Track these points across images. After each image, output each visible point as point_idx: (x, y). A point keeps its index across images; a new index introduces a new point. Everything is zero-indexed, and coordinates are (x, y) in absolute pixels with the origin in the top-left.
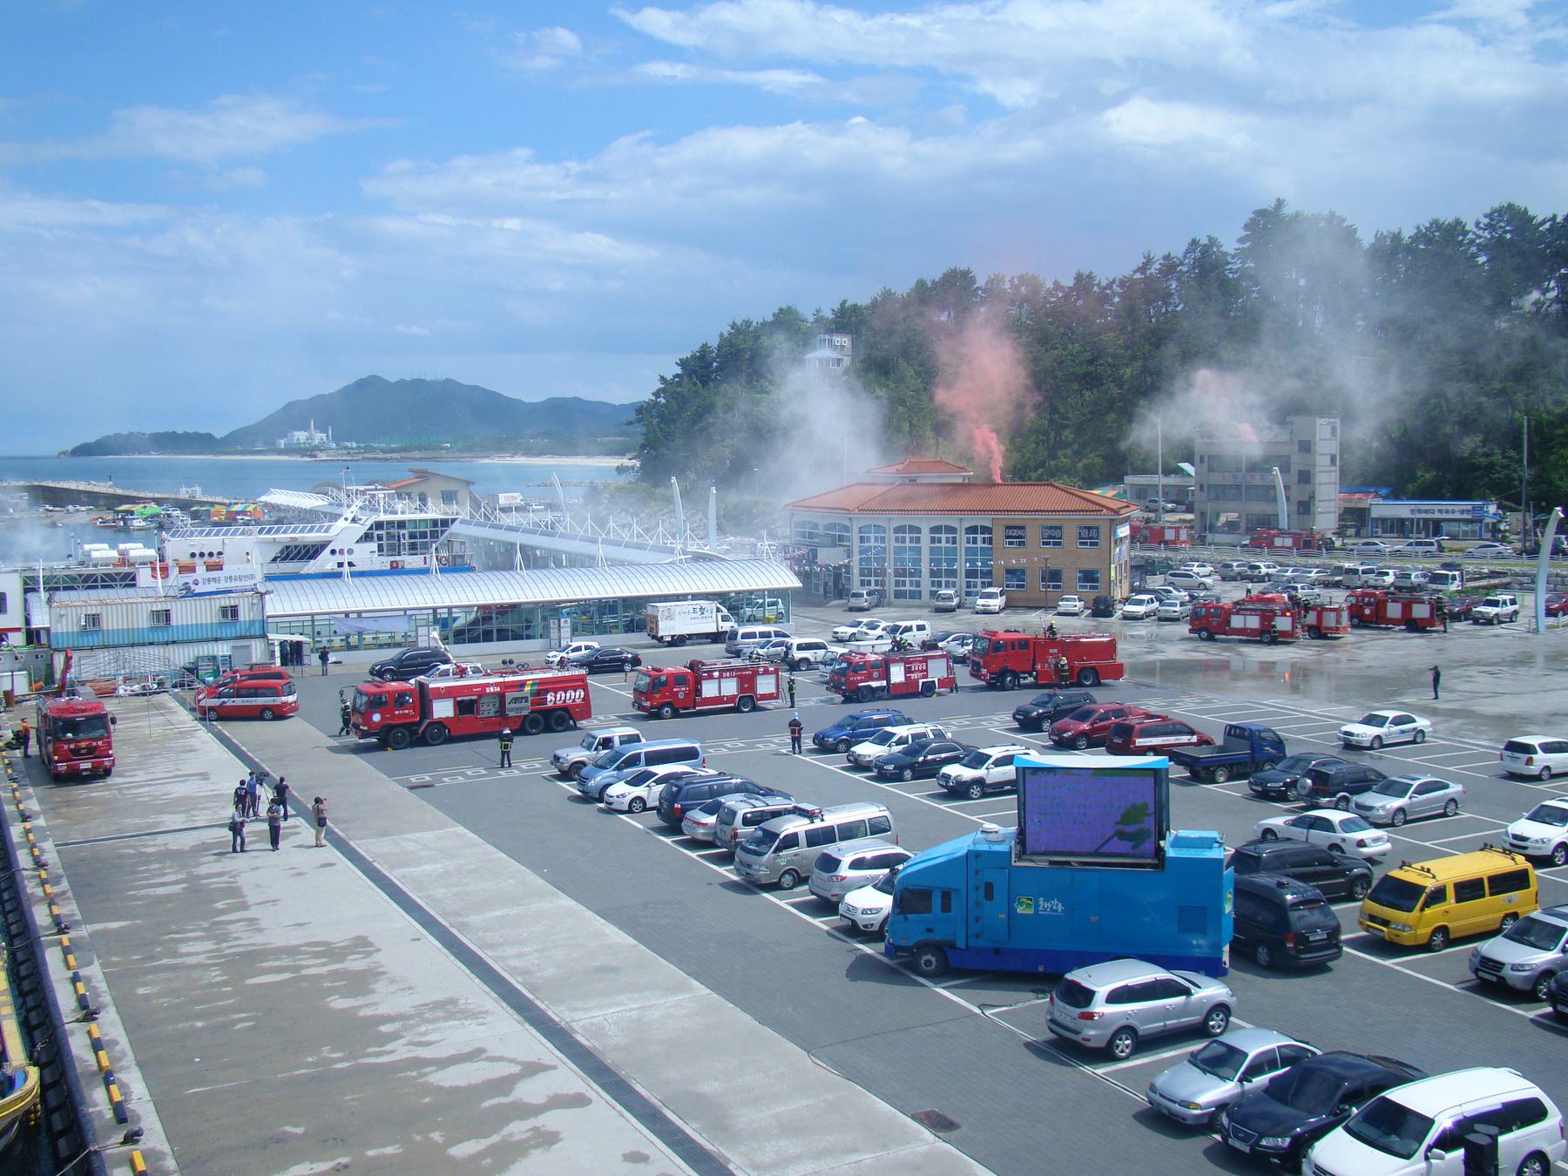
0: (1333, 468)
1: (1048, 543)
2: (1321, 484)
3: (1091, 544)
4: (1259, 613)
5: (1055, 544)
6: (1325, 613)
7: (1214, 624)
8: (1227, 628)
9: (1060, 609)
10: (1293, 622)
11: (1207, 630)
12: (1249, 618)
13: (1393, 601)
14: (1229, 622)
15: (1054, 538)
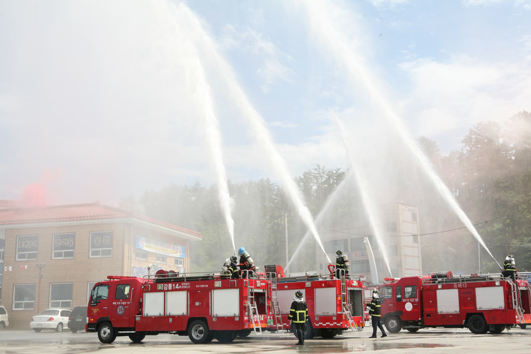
0: (416, 245)
1: (59, 255)
2: (405, 256)
3: (104, 252)
4: (186, 285)
5: (67, 254)
6: (318, 292)
7: (120, 311)
8: (138, 318)
9: (33, 324)
10: (242, 298)
11: (108, 323)
12: (171, 295)
13: (444, 287)
14: (141, 305)
15: (67, 248)
